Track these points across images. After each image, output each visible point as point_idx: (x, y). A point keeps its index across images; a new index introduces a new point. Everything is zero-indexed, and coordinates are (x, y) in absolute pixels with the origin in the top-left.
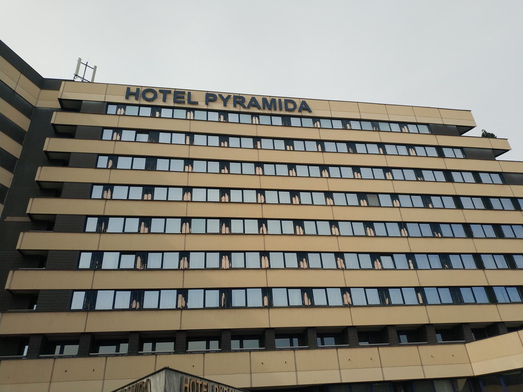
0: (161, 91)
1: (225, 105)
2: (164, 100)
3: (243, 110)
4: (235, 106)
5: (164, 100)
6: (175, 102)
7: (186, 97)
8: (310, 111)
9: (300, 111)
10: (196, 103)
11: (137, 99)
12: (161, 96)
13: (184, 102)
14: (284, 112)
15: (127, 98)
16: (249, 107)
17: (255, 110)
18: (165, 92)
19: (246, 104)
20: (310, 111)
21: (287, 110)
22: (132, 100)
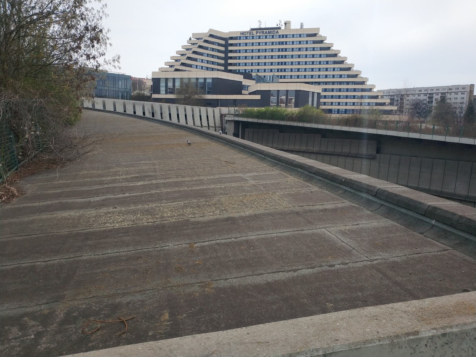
0: (247, 32)
1: (260, 34)
2: (248, 35)
3: (263, 35)
4: (262, 34)
5: (248, 35)
6: (250, 35)
7: (252, 33)
8: (278, 33)
9: (276, 33)
10: (254, 34)
11: (243, 35)
12: (247, 33)
13: (251, 35)
14: (273, 34)
15: (241, 35)
16: (265, 34)
17: (266, 34)
18: (248, 32)
19: (264, 33)
20: (278, 33)
21: (273, 34)
22: (242, 35)
